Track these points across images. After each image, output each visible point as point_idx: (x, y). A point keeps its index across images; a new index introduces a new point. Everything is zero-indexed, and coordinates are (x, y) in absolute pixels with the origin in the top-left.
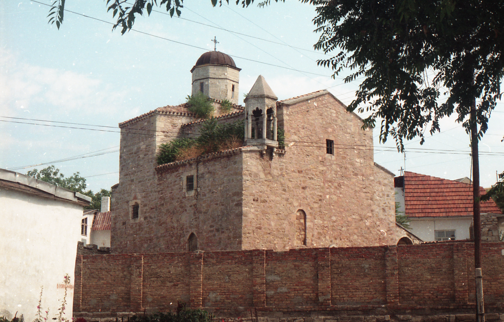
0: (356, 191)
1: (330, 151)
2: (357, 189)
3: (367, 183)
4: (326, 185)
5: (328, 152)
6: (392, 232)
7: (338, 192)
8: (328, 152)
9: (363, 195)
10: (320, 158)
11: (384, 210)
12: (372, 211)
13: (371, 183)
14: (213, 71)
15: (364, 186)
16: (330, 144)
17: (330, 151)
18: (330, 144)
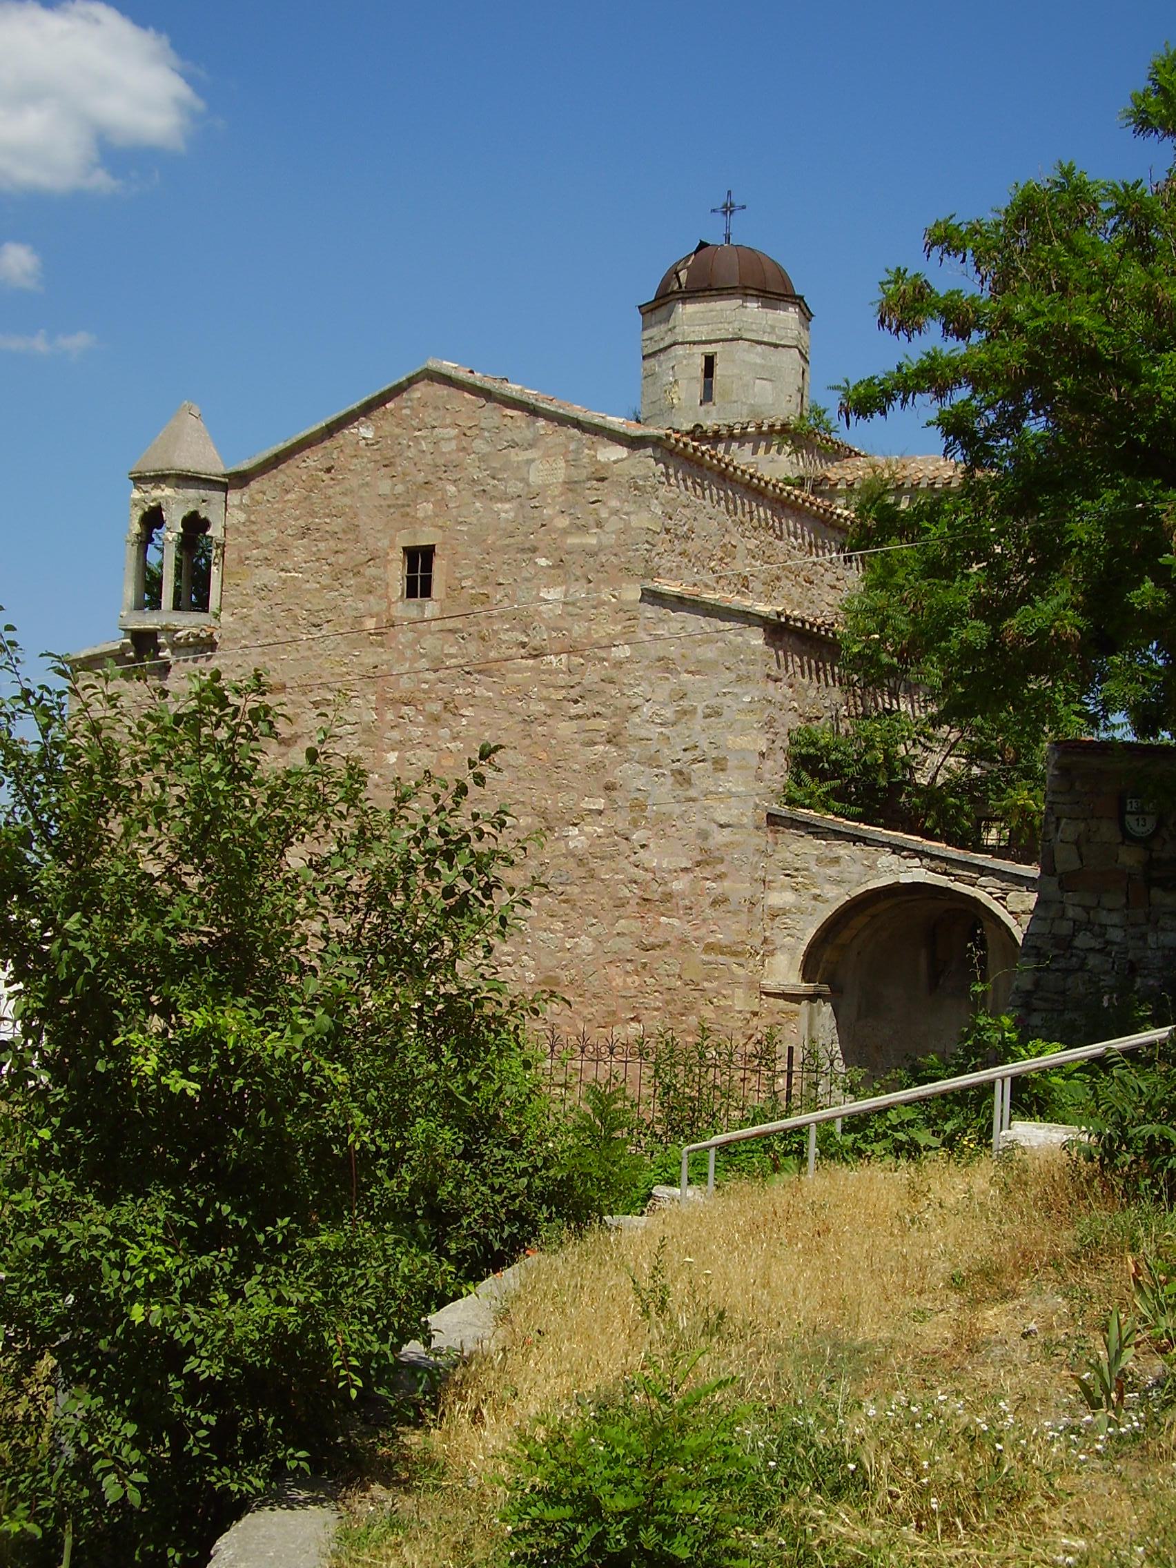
0: (529, 721)
1: (419, 586)
2: (538, 708)
3: (592, 676)
4: (390, 716)
5: (411, 593)
6: (721, 868)
7: (445, 732)
8: (411, 593)
9: (565, 728)
10: (370, 624)
11: (682, 778)
12: (609, 788)
13: (614, 673)
14: (691, 317)
15: (574, 693)
16: (420, 560)
17: (419, 586)
18: (420, 560)
